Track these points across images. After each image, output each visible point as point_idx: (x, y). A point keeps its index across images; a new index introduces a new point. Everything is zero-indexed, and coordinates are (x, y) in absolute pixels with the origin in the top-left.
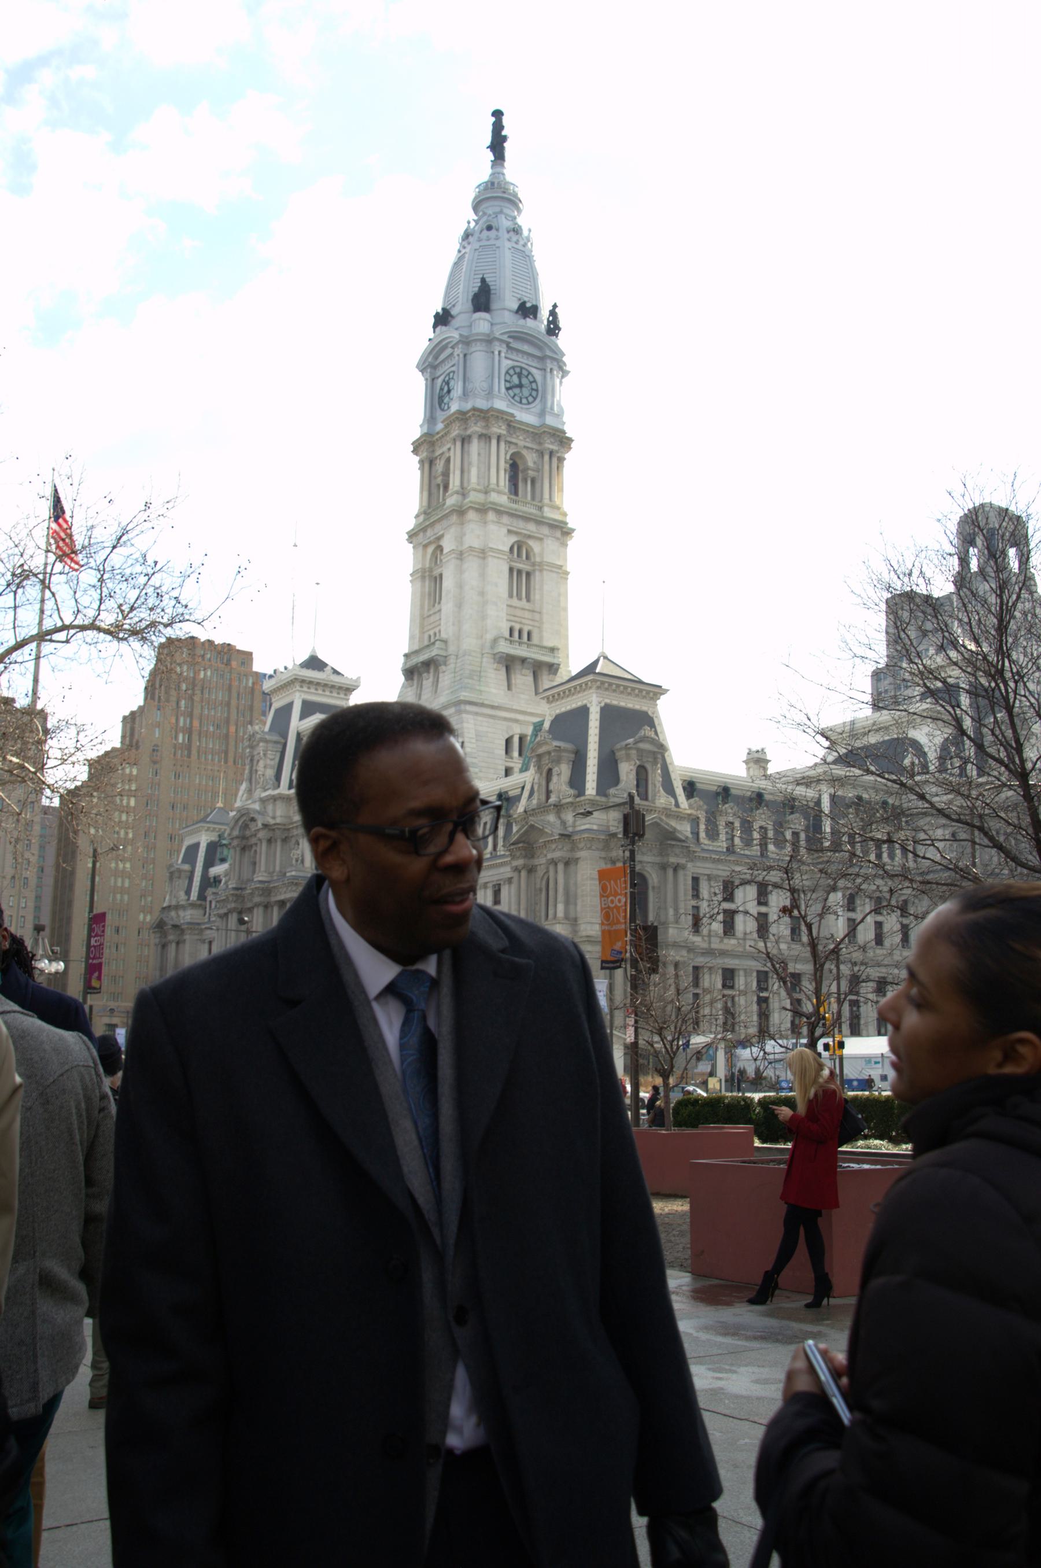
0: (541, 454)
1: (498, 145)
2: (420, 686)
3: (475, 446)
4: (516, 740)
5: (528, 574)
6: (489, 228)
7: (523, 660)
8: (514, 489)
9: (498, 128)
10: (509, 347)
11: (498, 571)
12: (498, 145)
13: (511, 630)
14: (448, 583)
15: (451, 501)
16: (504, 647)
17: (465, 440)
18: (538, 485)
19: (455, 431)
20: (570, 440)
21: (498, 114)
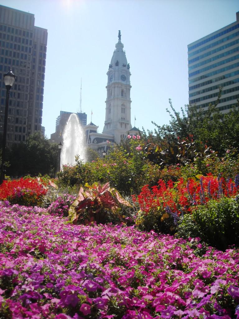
0: (126, 89)
1: (120, 36)
2: (107, 126)
3: (116, 88)
4: (122, 136)
5: (124, 109)
6: (118, 51)
7: (124, 123)
8: (122, 95)
9: (120, 33)
10: (121, 72)
11: (120, 109)
12: (120, 36)
13: (122, 118)
14: (112, 111)
15: (112, 97)
16: (120, 121)
17: (115, 87)
18: (126, 94)
19: (113, 86)
20: (131, 86)
21: (120, 31)
